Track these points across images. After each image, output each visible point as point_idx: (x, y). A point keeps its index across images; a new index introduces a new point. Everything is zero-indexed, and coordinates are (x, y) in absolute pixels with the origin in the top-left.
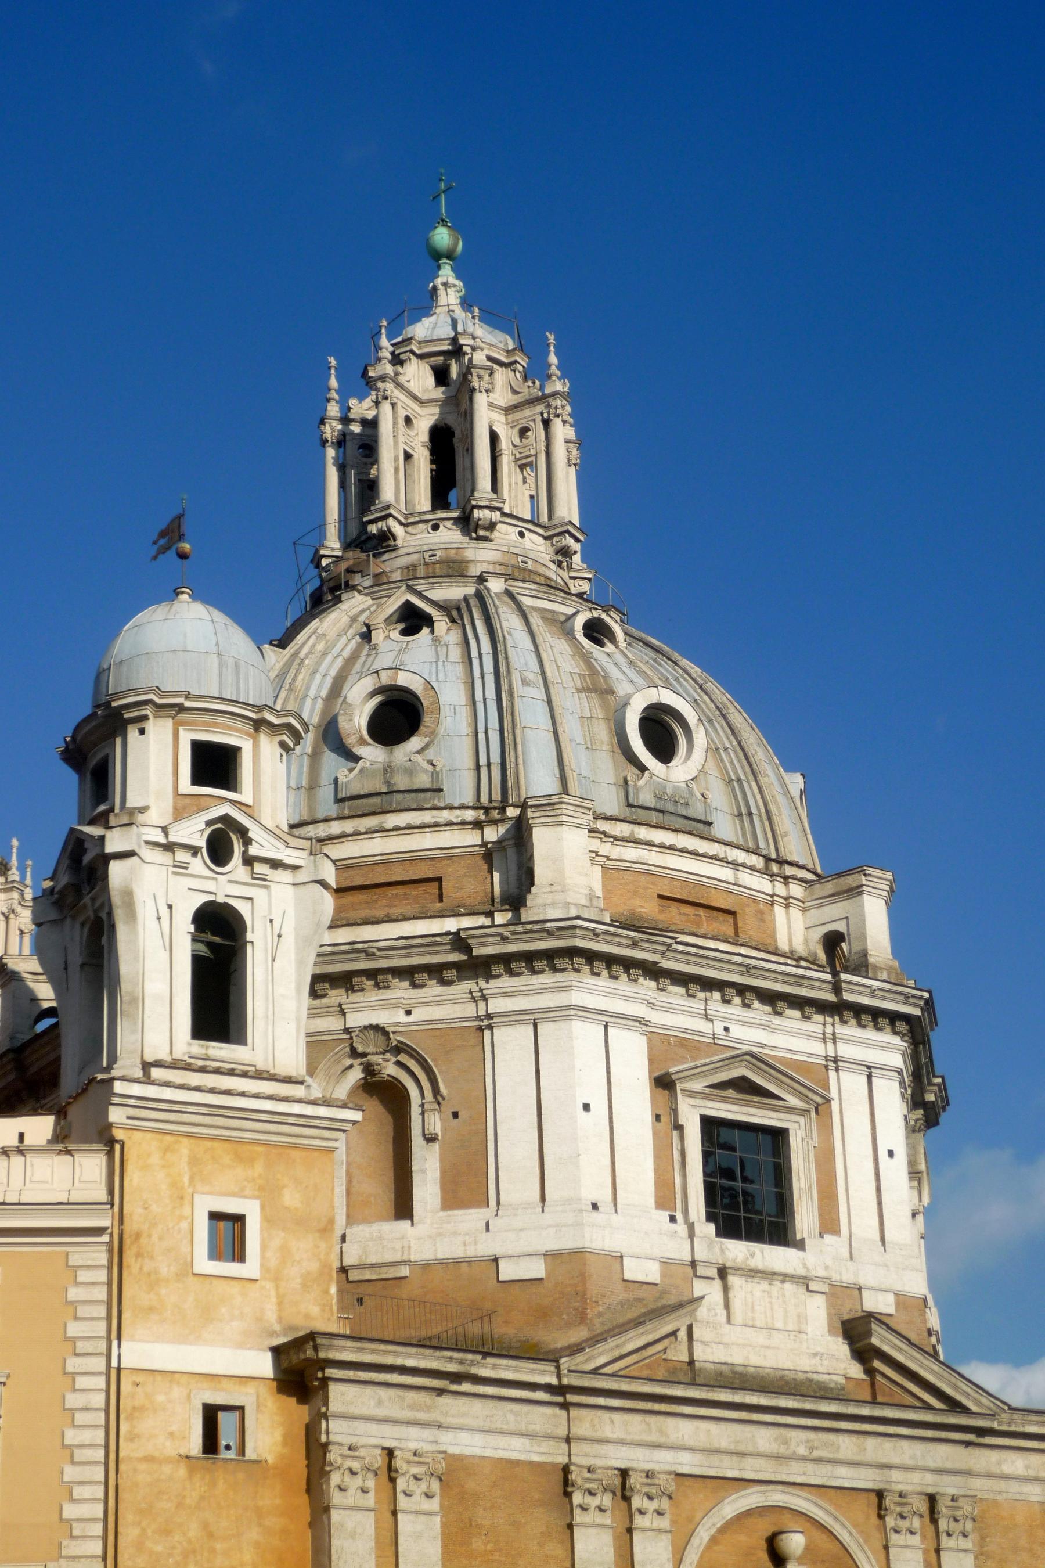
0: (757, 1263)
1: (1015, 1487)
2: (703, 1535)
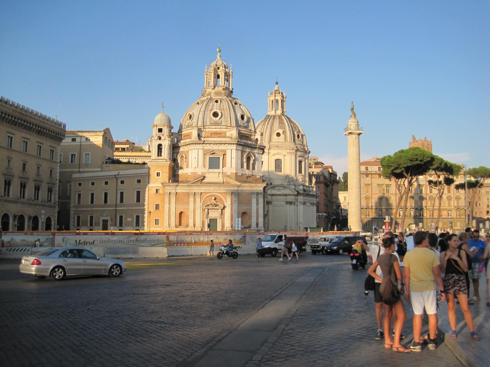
0: (213, 171)
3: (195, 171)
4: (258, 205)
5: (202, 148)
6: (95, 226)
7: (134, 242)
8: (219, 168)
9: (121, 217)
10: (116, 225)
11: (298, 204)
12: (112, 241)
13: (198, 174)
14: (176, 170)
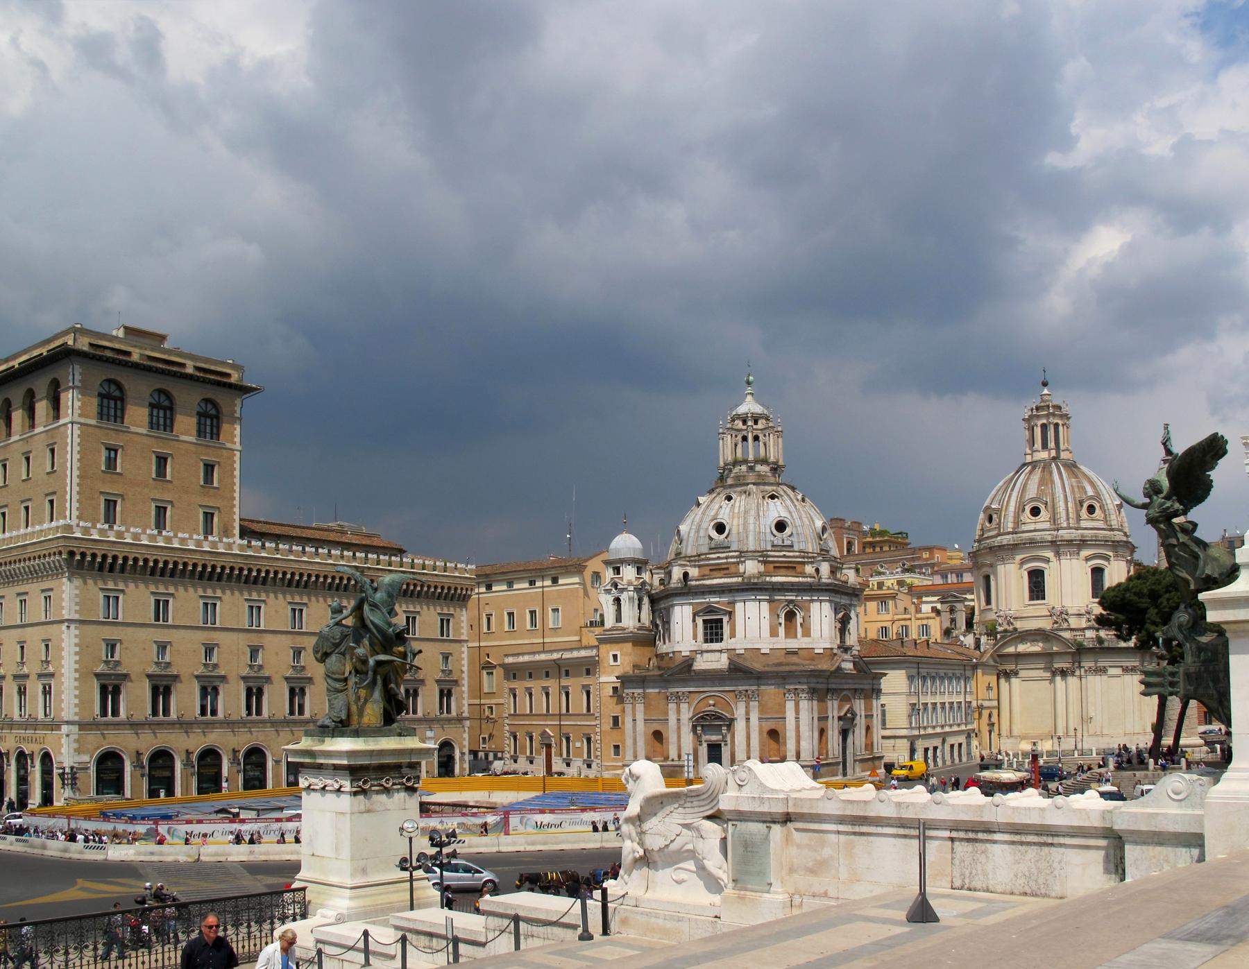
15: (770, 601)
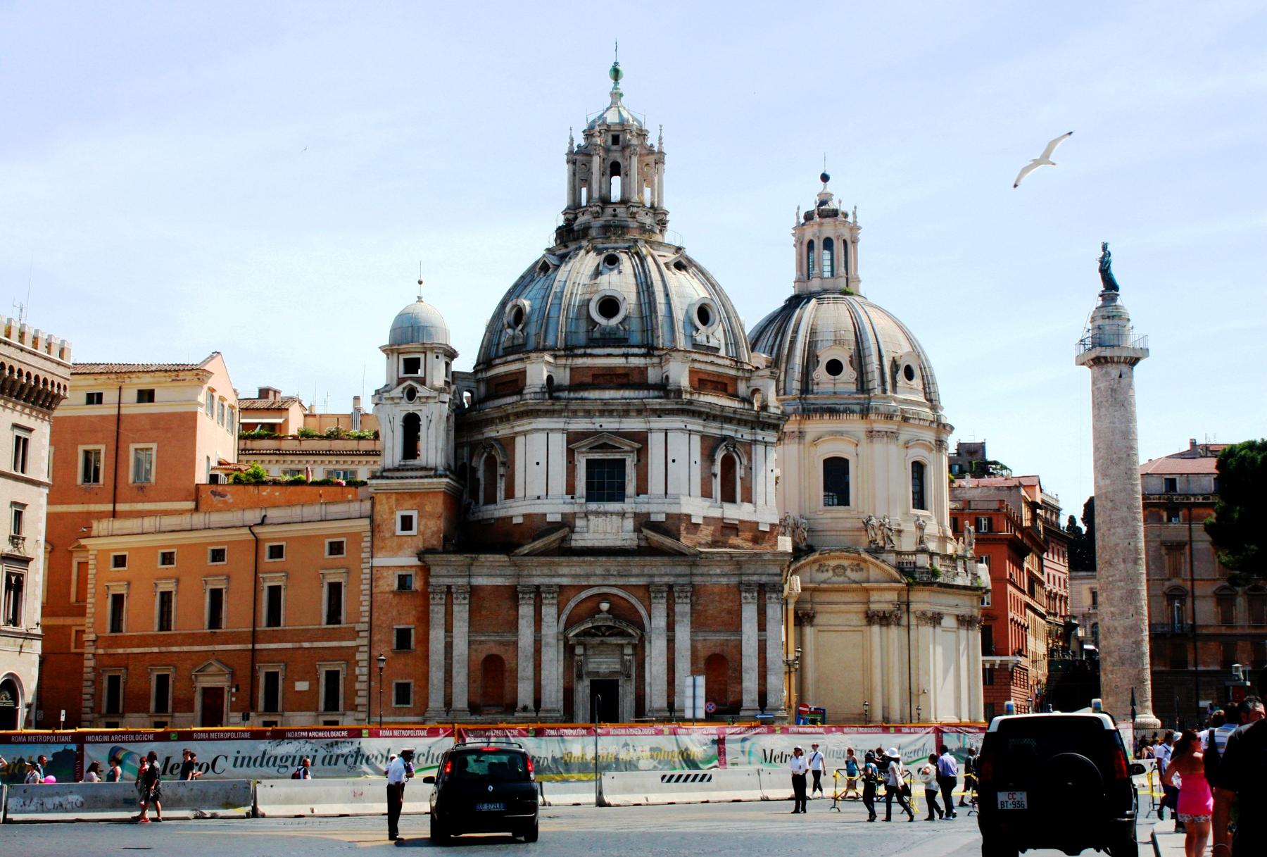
1: (714, 579)
2: (572, 604)
3: (537, 509)
4: (765, 630)
5: (561, 426)
6: (174, 711)
7: (350, 760)
8: (620, 496)
9: (272, 678)
10: (253, 707)
11: (913, 621)
12: (276, 758)
13: (550, 518)
14: (470, 504)
15: (704, 437)
